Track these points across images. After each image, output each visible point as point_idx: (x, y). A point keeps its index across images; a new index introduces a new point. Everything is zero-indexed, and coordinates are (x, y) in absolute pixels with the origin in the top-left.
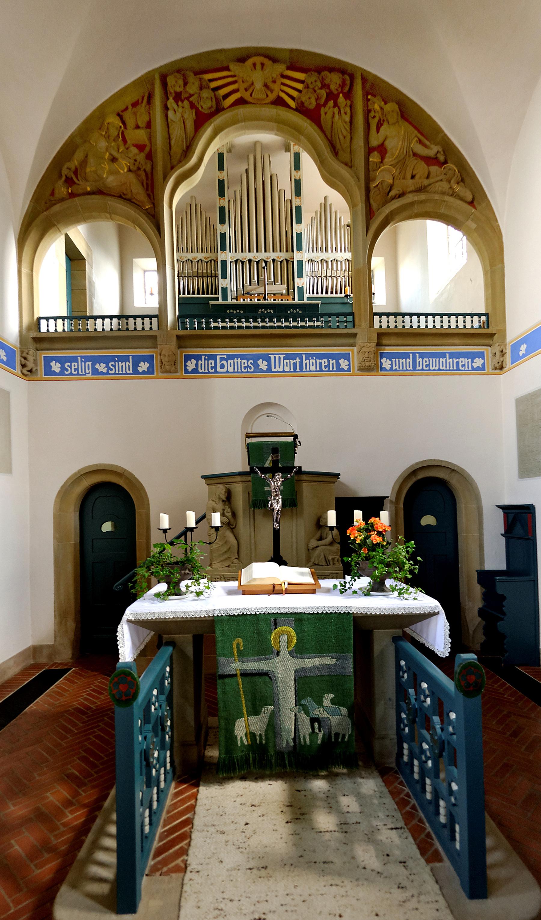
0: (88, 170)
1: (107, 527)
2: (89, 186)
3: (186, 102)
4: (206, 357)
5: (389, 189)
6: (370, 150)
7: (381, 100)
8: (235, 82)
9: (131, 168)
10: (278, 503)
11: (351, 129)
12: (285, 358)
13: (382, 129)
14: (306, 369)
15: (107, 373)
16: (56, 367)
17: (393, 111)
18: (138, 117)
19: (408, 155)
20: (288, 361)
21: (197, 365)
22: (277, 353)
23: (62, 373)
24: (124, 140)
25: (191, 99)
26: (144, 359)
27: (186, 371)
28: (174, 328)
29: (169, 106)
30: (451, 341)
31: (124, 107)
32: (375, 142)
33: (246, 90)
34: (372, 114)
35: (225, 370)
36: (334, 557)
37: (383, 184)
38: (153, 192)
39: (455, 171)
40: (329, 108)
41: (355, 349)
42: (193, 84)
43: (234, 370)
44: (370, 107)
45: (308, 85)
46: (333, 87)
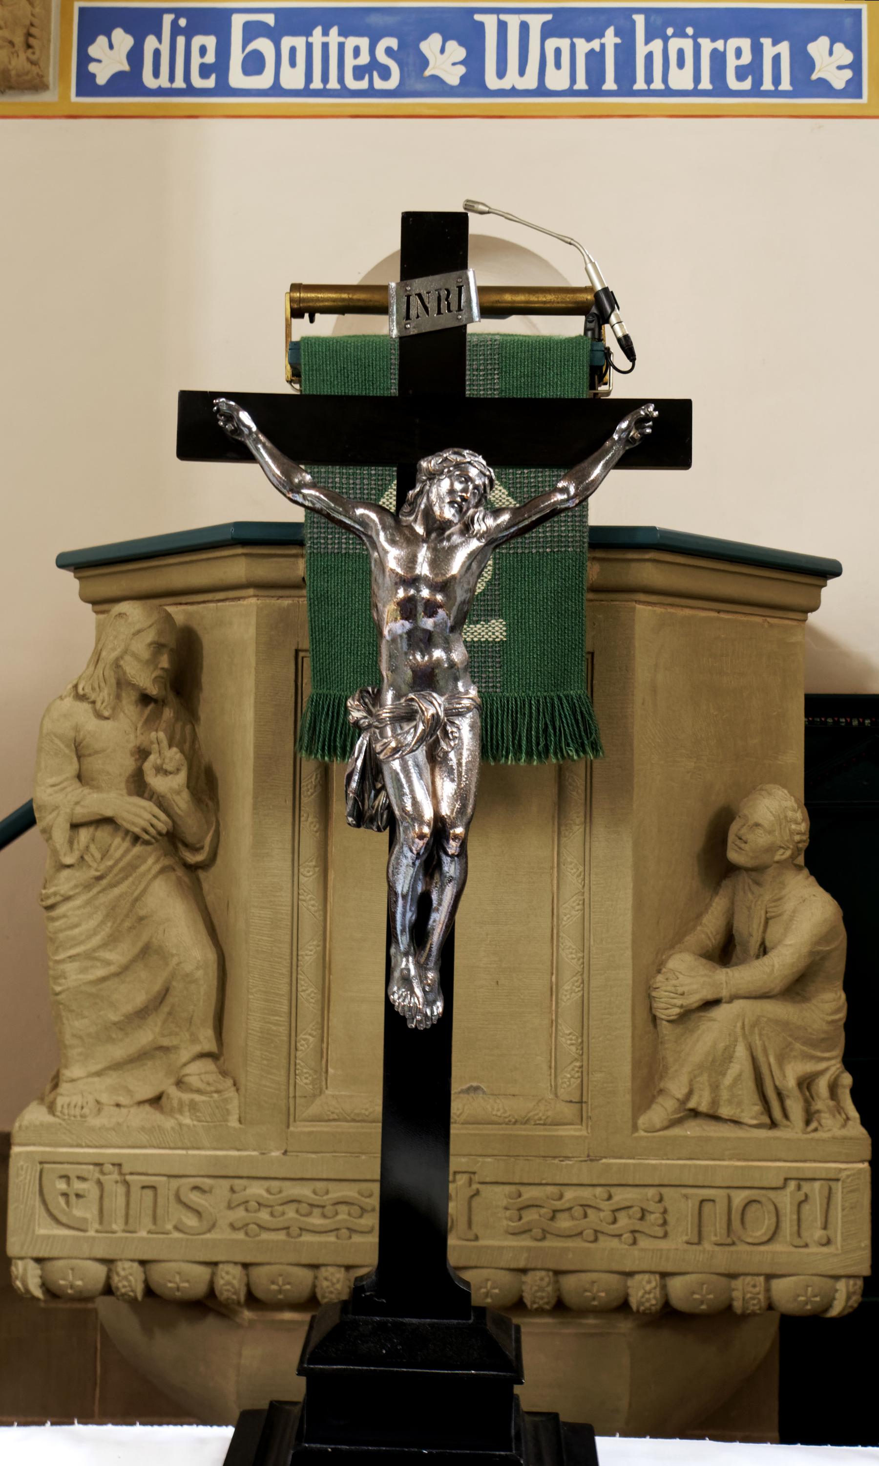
4: (183, 22)
10: (435, 758)
12: (547, 32)
14: (649, 79)
20: (564, 44)
21: (135, 56)
27: (87, 85)
35: (265, 80)
36: (809, 1067)
43: (309, 78)
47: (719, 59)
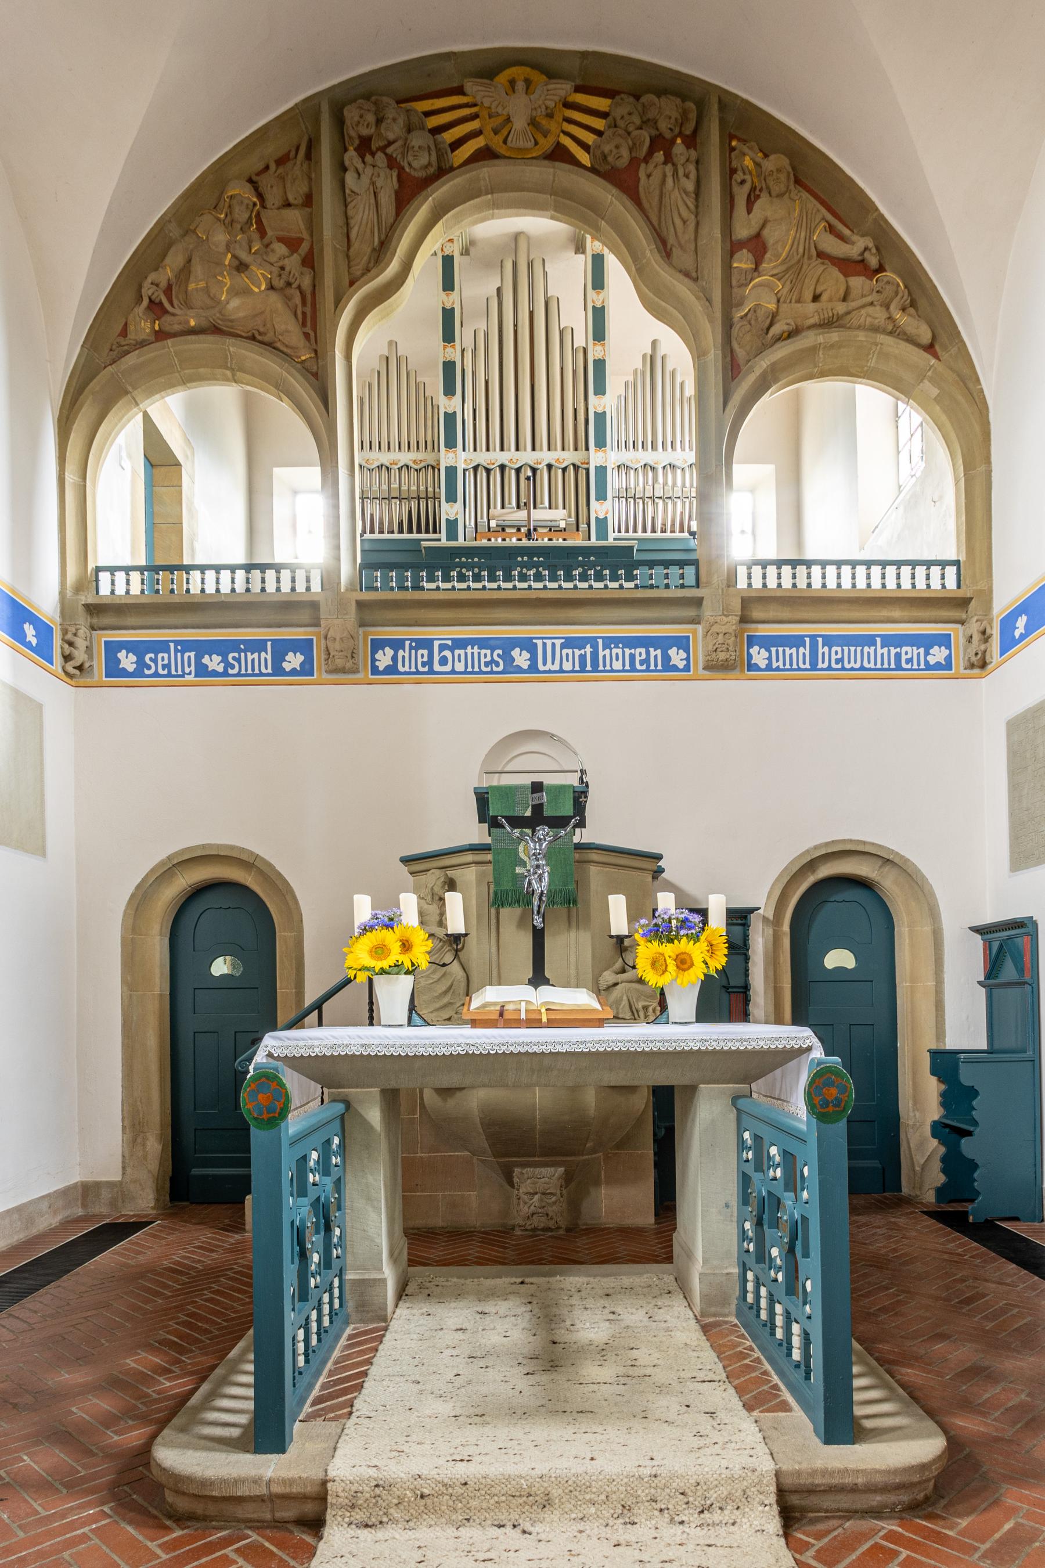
0: (192, 286)
1: (220, 967)
2: (193, 317)
3: (380, 155)
4: (414, 644)
5: (768, 321)
6: (733, 247)
7: (756, 148)
8: (475, 117)
9: (275, 283)
11: (697, 207)
12: (563, 646)
13: (757, 206)
14: (604, 666)
15: (225, 674)
16: (127, 661)
17: (779, 170)
18: (288, 185)
19: (806, 256)
20: (570, 651)
21: (394, 659)
22: (548, 635)
23: (138, 673)
24: (262, 231)
25: (389, 150)
26: (296, 646)
27: (375, 670)
28: (351, 588)
29: (347, 163)
30: (885, 613)
31: (261, 166)
32: (743, 231)
33: (496, 132)
34: (739, 177)
36: (647, 1003)
37: (758, 311)
38: (314, 328)
39: (898, 285)
40: (656, 167)
41: (700, 629)
42: (394, 120)
43: (466, 666)
44: (734, 164)
45: (615, 120)
46: (663, 126)
47: (632, 657)
